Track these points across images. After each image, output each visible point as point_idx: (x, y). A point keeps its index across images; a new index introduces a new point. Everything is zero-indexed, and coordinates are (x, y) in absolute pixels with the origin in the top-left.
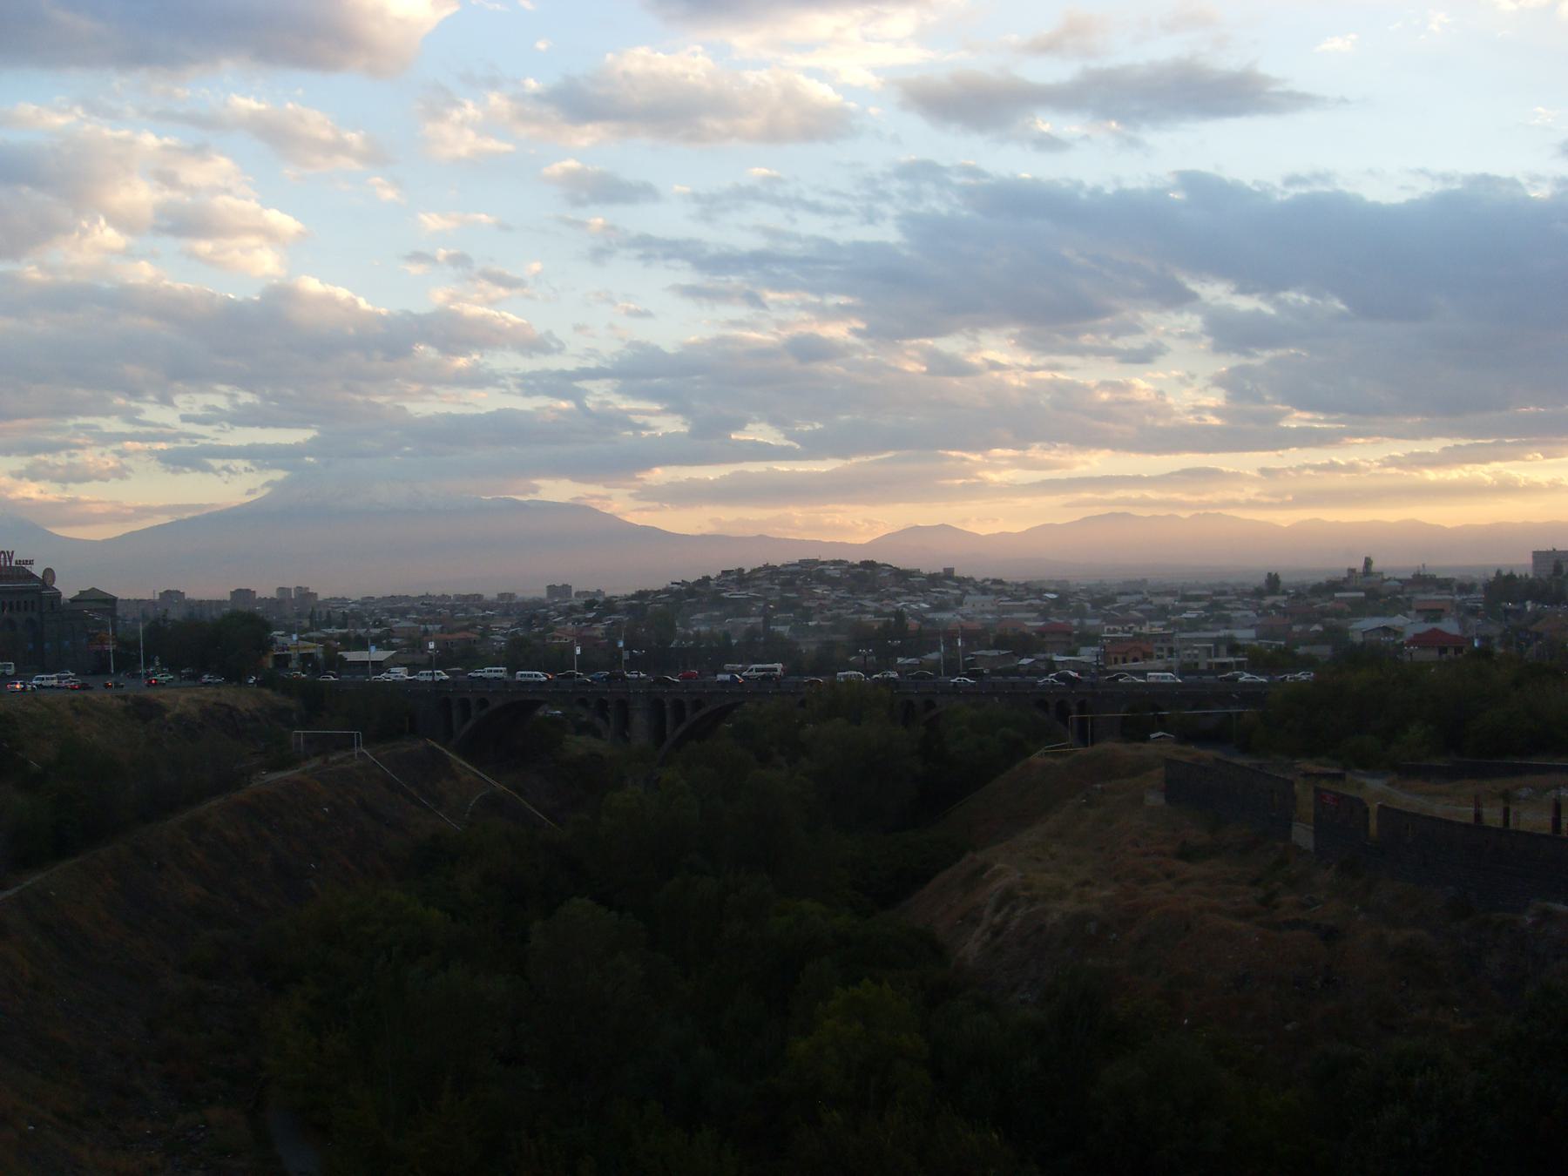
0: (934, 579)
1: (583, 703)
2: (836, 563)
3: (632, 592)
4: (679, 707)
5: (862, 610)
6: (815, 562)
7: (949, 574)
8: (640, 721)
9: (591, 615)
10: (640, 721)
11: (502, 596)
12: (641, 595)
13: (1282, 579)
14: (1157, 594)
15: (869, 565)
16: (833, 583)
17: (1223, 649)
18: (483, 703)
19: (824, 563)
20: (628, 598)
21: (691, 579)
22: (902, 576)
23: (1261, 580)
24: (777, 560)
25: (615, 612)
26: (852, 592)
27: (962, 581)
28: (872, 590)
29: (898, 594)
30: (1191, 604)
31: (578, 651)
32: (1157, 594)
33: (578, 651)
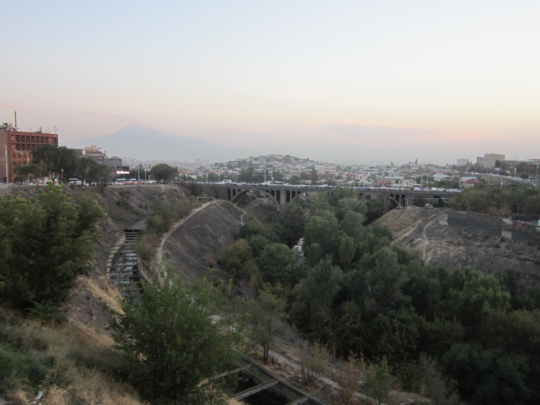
0: (304, 160)
2: (279, 155)
4: (294, 193)
5: (288, 168)
6: (275, 155)
7: (308, 160)
8: (283, 197)
10: (283, 197)
11: (185, 161)
15: (287, 156)
16: (280, 160)
17: (416, 182)
18: (239, 190)
22: (297, 159)
25: (223, 166)
26: (285, 163)
27: (312, 161)
28: (290, 163)
29: (295, 164)
30: (374, 169)
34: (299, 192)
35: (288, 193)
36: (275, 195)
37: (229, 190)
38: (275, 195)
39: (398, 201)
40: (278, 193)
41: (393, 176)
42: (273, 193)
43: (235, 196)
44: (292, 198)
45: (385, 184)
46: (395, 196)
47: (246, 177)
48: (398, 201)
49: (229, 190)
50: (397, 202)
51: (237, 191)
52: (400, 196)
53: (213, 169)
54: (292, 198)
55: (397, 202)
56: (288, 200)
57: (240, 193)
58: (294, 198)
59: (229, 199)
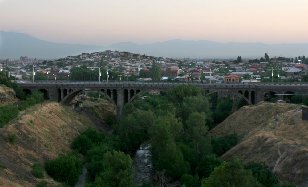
1: (103, 90)
3: (58, 58)
4: (132, 91)
6: (110, 51)
8: (120, 96)
9: (45, 65)
10: (120, 96)
12: (60, 60)
13: (242, 58)
14: (206, 62)
18: (70, 90)
19: (112, 52)
20: (57, 61)
21: (74, 55)
23: (236, 58)
24: (99, 51)
31: (100, 75)
32: (206, 62)
33: (100, 75)
34: (138, 91)
35: (126, 92)
36: (112, 95)
37: (59, 91)
38: (112, 95)
39: (248, 99)
40: (115, 92)
41: (241, 71)
42: (109, 92)
43: (66, 97)
44: (131, 98)
45: (233, 80)
46: (244, 93)
47: (77, 75)
48: (248, 99)
49: (59, 91)
50: (246, 99)
51: (68, 91)
52: (250, 93)
53: (42, 67)
54: (131, 98)
55: (246, 99)
56: (126, 100)
57: (71, 93)
58: (133, 98)
59: (59, 100)
